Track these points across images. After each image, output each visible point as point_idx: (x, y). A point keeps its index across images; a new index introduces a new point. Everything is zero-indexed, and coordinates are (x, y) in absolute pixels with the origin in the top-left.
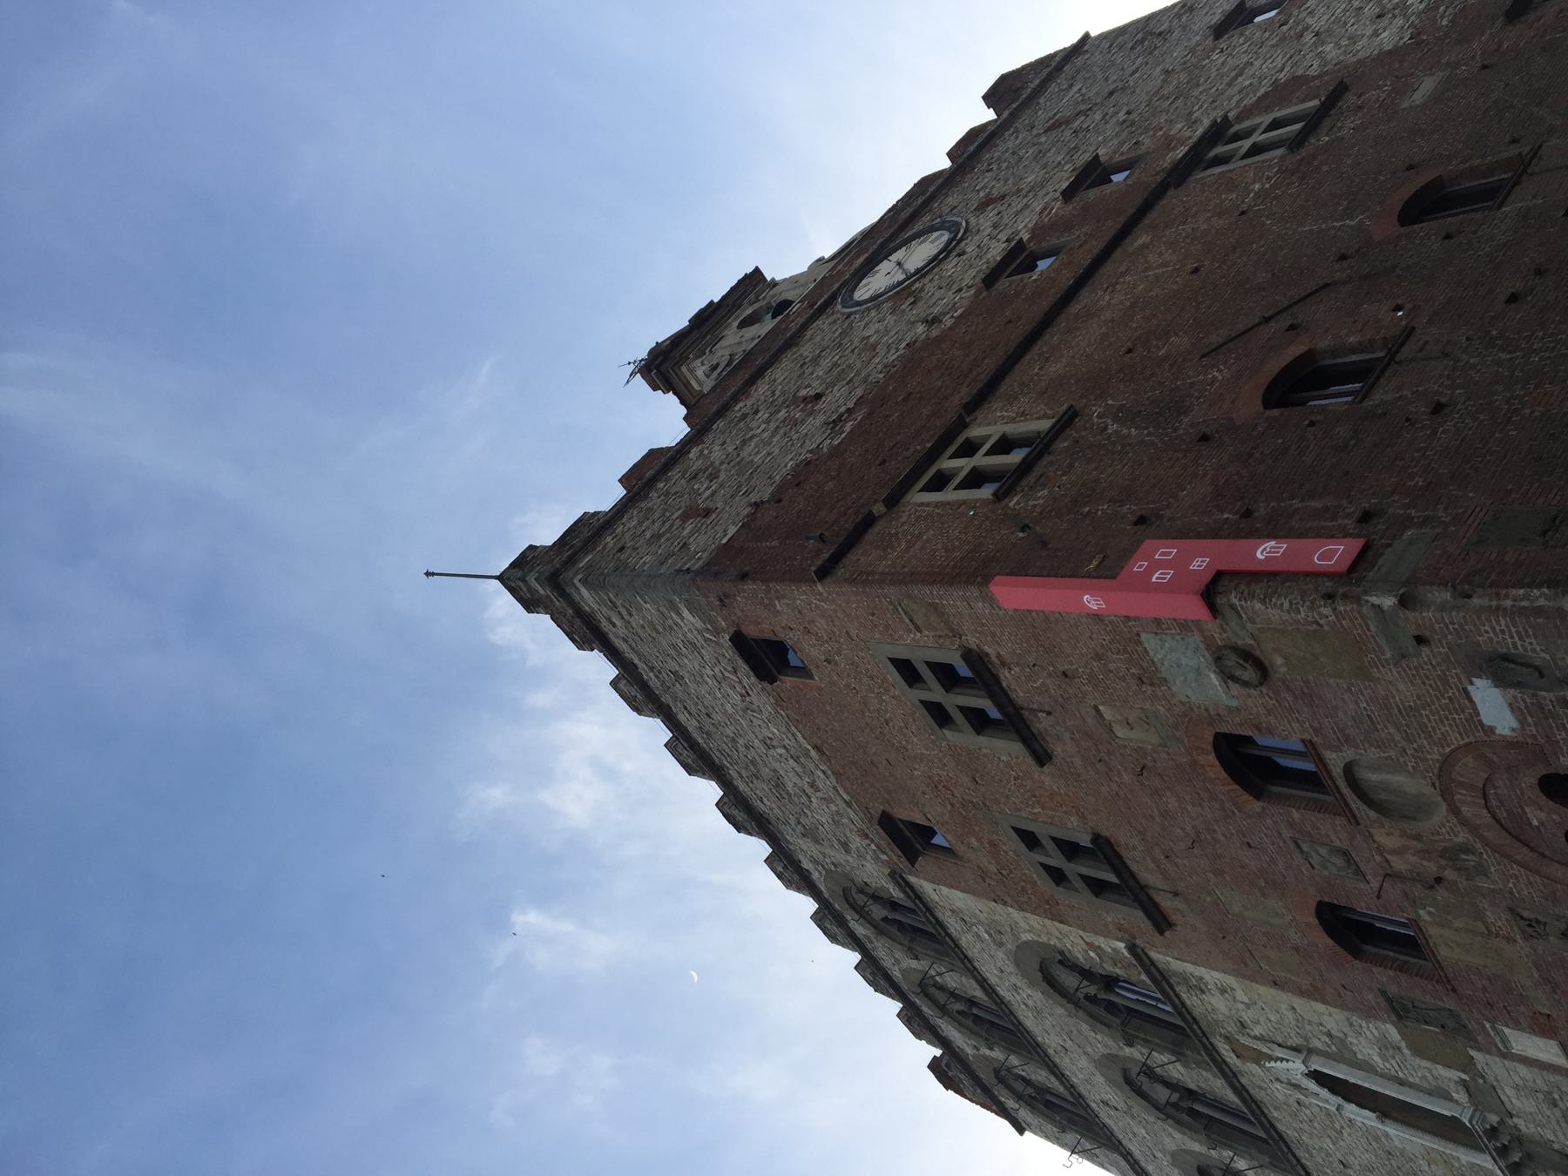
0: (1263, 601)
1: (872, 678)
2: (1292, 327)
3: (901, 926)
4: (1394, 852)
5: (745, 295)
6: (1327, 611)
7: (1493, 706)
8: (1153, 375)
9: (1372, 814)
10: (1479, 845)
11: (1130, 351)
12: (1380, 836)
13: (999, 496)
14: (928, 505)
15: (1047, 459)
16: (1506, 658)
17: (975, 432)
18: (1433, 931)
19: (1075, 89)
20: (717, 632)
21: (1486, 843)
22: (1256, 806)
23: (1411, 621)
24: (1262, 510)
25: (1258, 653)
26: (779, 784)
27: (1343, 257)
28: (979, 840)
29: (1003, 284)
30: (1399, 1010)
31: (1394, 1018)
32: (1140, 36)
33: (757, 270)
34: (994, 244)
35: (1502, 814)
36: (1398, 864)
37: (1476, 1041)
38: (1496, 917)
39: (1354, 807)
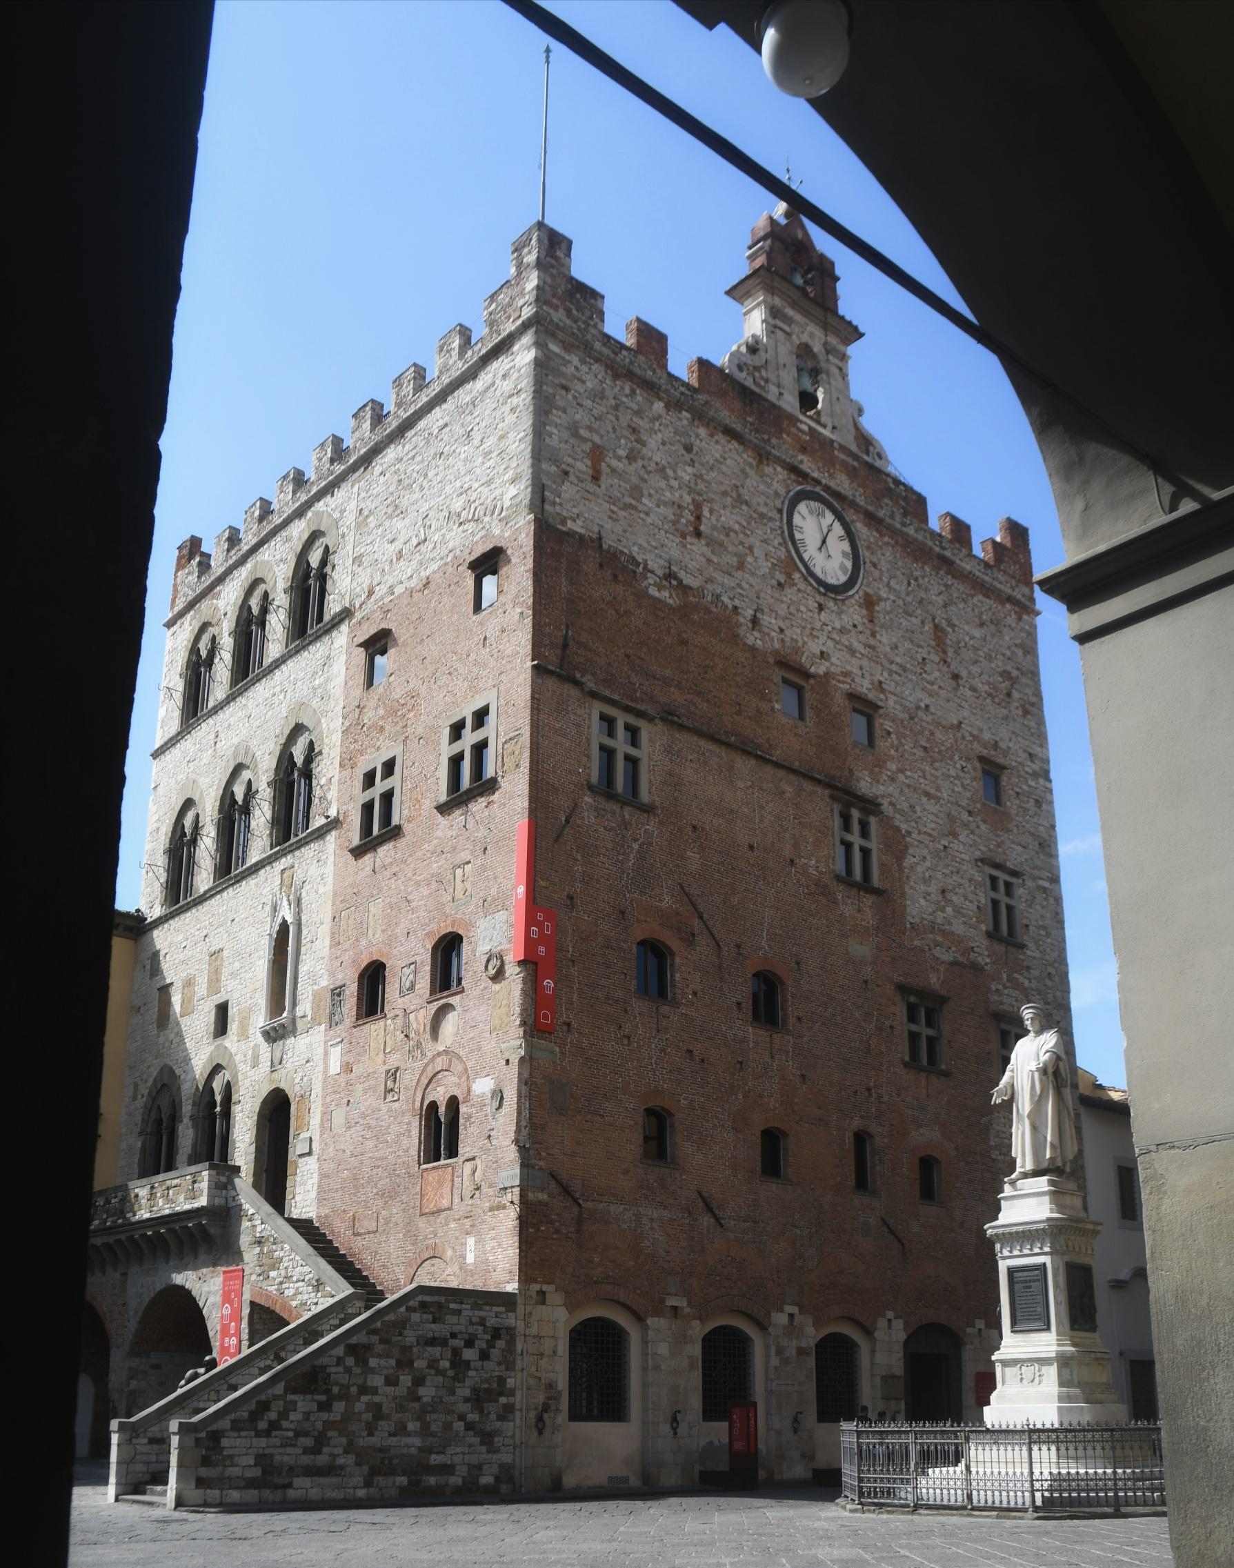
2: (693, 935)
3: (307, 576)
5: (836, 332)
7: (483, 1086)
8: (672, 855)
10: (425, 1061)
11: (694, 827)
12: (422, 1012)
13: (591, 788)
14: (589, 727)
15: (616, 807)
16: (502, 1098)
17: (646, 732)
19: (977, 633)
21: (427, 1065)
22: (430, 947)
23: (515, 1060)
24: (574, 971)
26: (397, 510)
27: (738, 946)
28: (382, 718)
29: (777, 675)
32: (1015, 673)
34: (823, 639)
35: (440, 1076)
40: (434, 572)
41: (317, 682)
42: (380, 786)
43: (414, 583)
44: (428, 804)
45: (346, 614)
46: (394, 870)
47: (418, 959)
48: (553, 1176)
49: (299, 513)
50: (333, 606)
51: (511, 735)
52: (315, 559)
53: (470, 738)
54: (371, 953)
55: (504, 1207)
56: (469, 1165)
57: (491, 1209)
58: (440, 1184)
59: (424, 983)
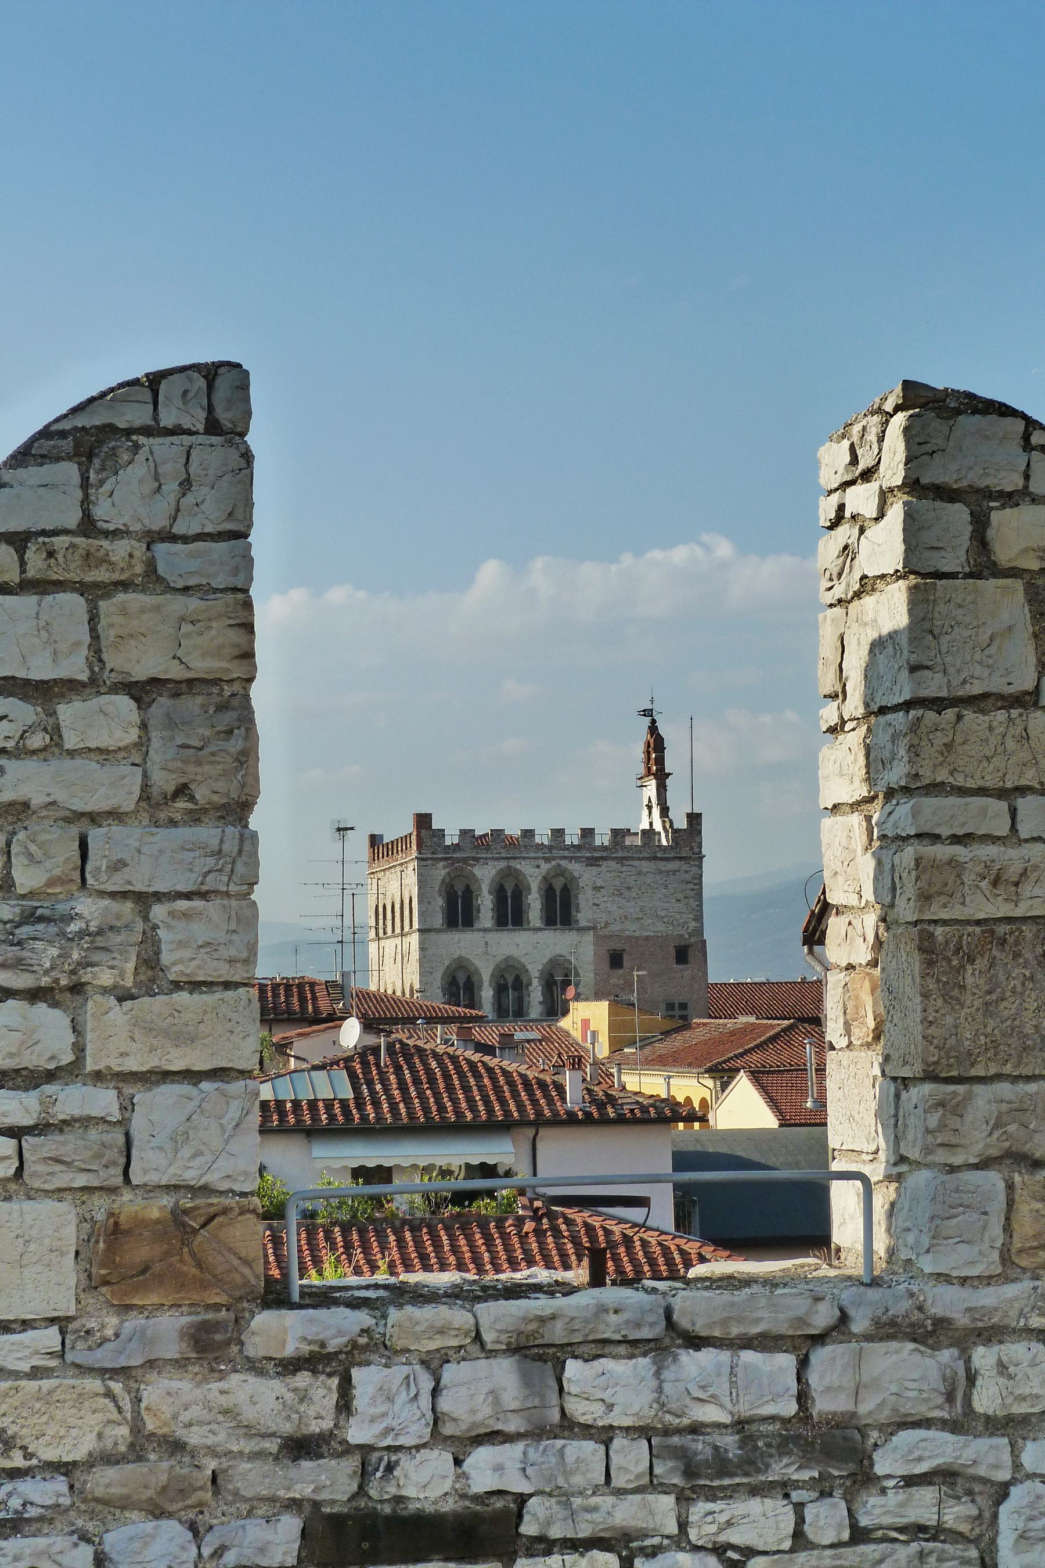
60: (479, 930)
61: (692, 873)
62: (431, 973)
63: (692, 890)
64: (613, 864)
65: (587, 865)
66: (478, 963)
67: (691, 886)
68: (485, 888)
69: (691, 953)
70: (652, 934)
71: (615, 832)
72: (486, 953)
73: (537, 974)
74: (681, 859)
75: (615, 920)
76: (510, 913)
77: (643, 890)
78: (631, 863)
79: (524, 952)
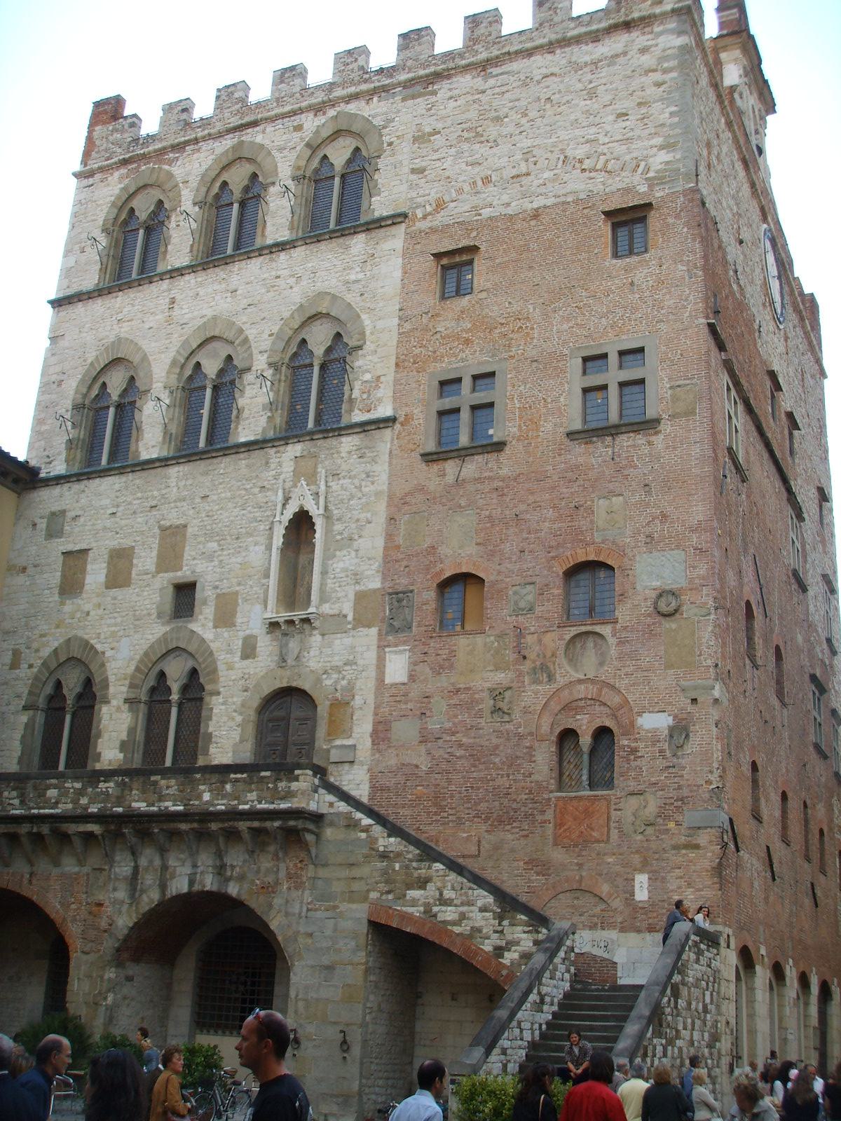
0: (712, 632)
1: (622, 318)
4: (540, 641)
6: (709, 662)
7: (655, 722)
9: (568, 637)
10: (555, 686)
16: (687, 736)
18: (479, 640)
20: (651, 183)
25: (677, 615)
26: (477, 136)
28: (469, 330)
29: (768, 384)
30: (399, 597)
31: (391, 591)
33: (774, 112)
35: (582, 703)
36: (530, 639)
37: (387, 634)
38: (501, 678)
39: (572, 629)
40: (545, 207)
41: (353, 277)
42: (466, 396)
43: (510, 211)
44: (551, 429)
45: (399, 218)
46: (497, 484)
47: (538, 580)
48: (731, 820)
49: (318, 109)
50: (380, 206)
51: (678, 383)
52: (339, 155)
53: (613, 375)
54: (460, 564)
55: (697, 847)
56: (634, 801)
57: (676, 847)
58: (588, 813)
59: (551, 608)
60: (162, 277)
61: (657, 52)
62: (60, 383)
63: (658, 85)
64: (465, 82)
65: (404, 100)
66: (149, 346)
67: (657, 77)
68: (187, 199)
69: (654, 220)
70: (549, 202)
71: (473, 21)
72: (169, 320)
73: (266, 343)
74: (627, 25)
75: (460, 191)
76: (232, 229)
77: (532, 114)
78: (505, 68)
79: (245, 302)
